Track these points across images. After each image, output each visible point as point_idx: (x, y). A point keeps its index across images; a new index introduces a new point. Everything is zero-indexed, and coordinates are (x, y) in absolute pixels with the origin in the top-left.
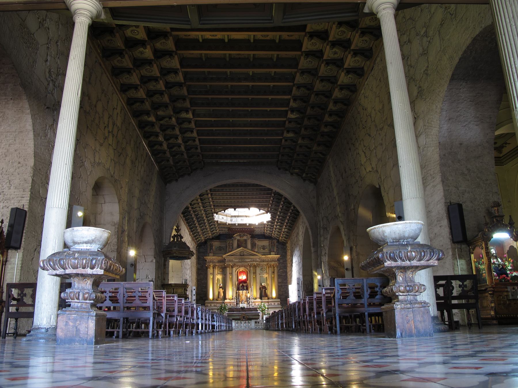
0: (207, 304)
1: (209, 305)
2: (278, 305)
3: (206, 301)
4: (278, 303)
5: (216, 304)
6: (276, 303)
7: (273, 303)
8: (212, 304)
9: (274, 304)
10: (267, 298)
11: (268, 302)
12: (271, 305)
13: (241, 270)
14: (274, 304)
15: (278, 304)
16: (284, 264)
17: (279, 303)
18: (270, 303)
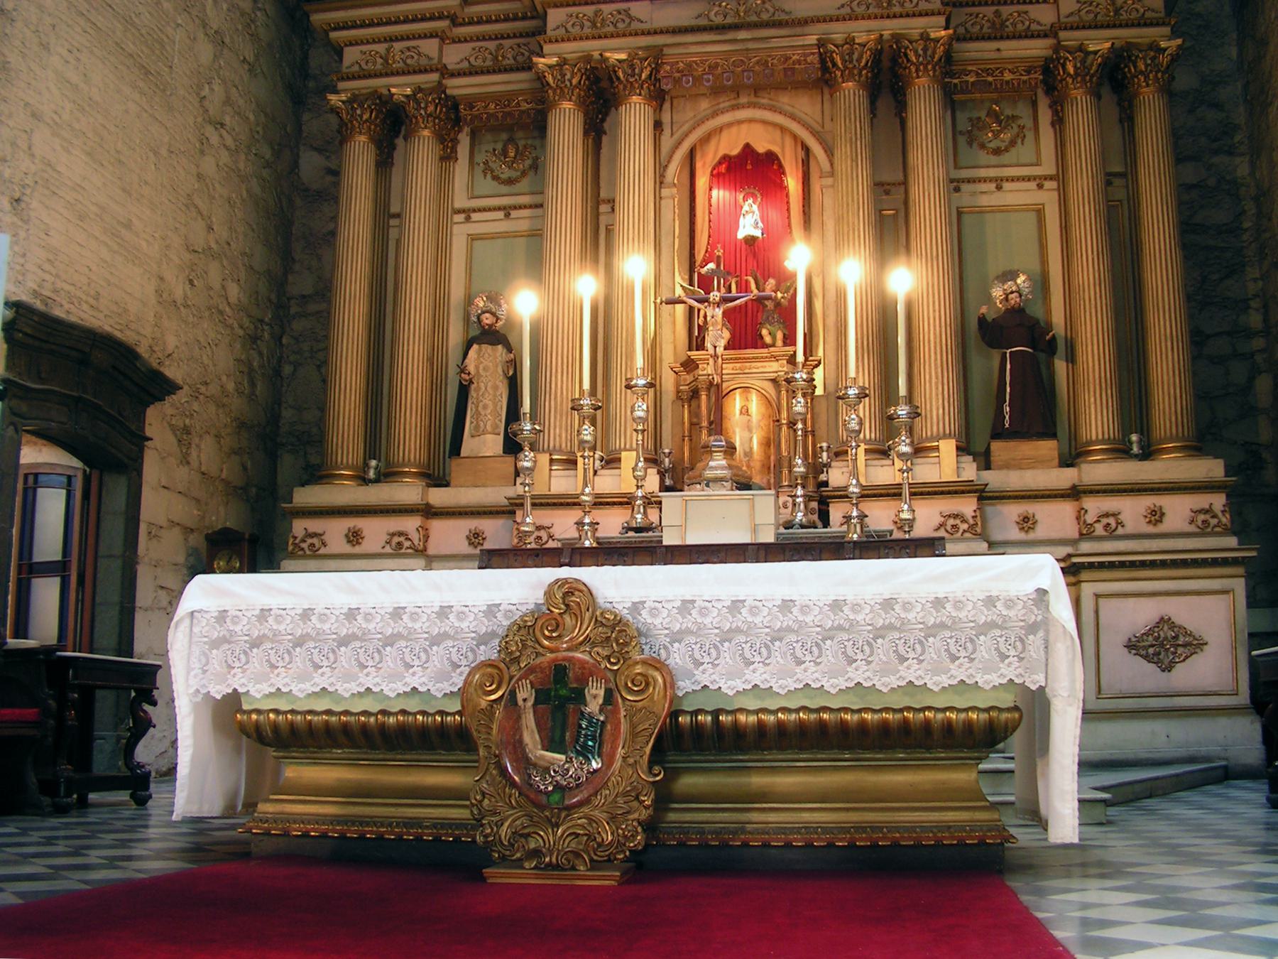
0: (314, 525)
1: (335, 530)
2: (1204, 531)
3: (307, 496)
4: (1202, 500)
5: (411, 524)
6: (1178, 510)
7: (1132, 510)
8: (365, 524)
9: (1156, 516)
10: (1048, 448)
11: (1075, 493)
12: (1111, 535)
13: (730, 144)
14: (1156, 516)
15: (1203, 524)
16: (1217, 106)
17: (1218, 501)
18: (1094, 506)
